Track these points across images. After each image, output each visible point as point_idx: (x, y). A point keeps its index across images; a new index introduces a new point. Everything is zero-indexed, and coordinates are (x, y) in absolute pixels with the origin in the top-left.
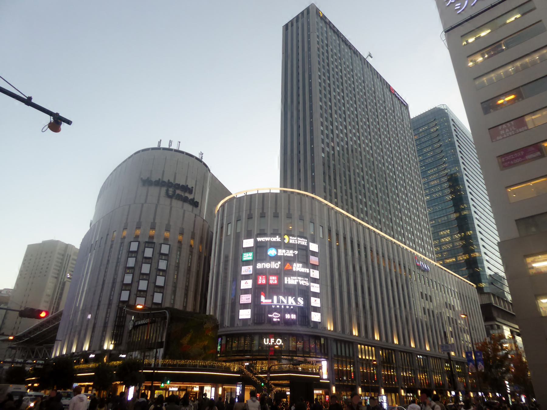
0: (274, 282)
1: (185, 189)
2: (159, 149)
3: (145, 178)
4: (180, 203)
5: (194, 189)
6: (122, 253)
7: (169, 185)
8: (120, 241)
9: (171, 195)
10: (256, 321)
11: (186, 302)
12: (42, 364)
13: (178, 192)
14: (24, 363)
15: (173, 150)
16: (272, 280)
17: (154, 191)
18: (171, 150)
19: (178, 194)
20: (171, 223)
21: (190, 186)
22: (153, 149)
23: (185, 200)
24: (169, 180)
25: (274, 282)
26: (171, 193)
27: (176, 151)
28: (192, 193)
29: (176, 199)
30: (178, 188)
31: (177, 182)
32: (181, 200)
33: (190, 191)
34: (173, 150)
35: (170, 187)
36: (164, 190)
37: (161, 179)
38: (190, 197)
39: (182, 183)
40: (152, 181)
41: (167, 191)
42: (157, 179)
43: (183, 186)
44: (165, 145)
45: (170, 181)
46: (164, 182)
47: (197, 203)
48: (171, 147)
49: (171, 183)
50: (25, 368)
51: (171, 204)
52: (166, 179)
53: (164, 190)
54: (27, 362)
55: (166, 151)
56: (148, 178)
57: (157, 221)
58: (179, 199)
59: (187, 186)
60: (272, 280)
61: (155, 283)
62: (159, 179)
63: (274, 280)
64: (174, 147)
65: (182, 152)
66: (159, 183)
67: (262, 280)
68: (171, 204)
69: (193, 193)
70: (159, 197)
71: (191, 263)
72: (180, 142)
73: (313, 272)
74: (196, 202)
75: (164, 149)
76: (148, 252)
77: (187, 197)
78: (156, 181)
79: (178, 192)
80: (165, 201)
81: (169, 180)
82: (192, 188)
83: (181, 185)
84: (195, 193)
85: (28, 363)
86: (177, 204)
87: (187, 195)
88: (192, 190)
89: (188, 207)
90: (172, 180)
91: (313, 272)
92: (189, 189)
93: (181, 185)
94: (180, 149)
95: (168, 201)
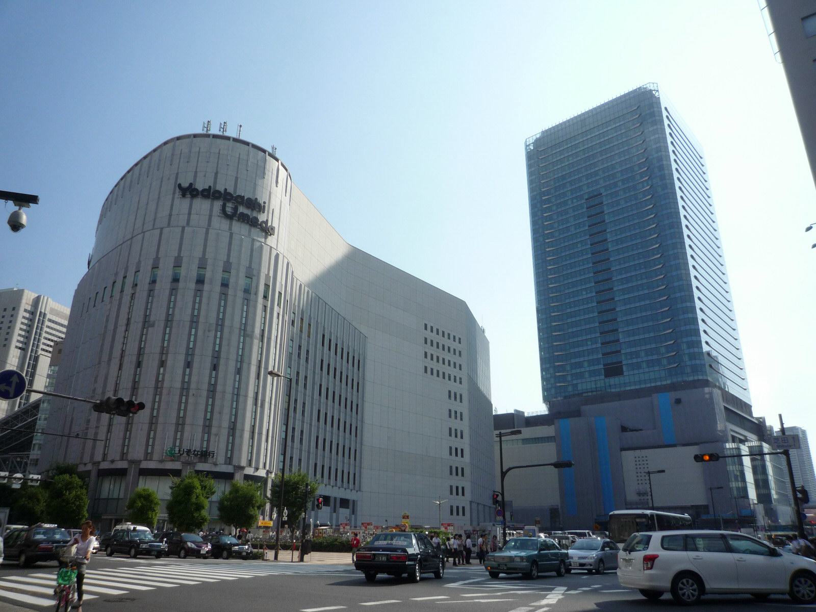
2: (208, 136)
3: (185, 185)
5: (266, 205)
6: (151, 308)
7: (226, 196)
8: (146, 287)
9: (229, 213)
12: (37, 480)
13: (241, 209)
14: (10, 478)
15: (231, 139)
17: (202, 206)
18: (228, 138)
19: (242, 214)
22: (195, 136)
24: (226, 190)
26: (229, 210)
27: (235, 140)
29: (239, 220)
31: (239, 192)
32: (248, 223)
34: (231, 139)
35: (229, 200)
36: (218, 204)
40: (197, 190)
41: (224, 206)
42: (207, 188)
43: (249, 199)
46: (219, 192)
48: (226, 134)
49: (230, 194)
50: (11, 486)
51: (230, 229)
52: (220, 188)
53: (218, 204)
54: (14, 476)
55: (219, 141)
56: (191, 184)
57: (209, 255)
58: (243, 221)
59: (256, 199)
62: (210, 187)
64: (231, 132)
65: (247, 144)
66: (209, 194)
68: (230, 229)
69: (266, 212)
70: (210, 216)
72: (241, 126)
75: (215, 136)
78: (204, 190)
79: (241, 209)
80: (220, 224)
81: (226, 190)
82: (265, 203)
85: (15, 478)
87: (255, 214)
88: (264, 206)
90: (231, 190)
92: (259, 205)
94: (242, 138)
95: (225, 224)
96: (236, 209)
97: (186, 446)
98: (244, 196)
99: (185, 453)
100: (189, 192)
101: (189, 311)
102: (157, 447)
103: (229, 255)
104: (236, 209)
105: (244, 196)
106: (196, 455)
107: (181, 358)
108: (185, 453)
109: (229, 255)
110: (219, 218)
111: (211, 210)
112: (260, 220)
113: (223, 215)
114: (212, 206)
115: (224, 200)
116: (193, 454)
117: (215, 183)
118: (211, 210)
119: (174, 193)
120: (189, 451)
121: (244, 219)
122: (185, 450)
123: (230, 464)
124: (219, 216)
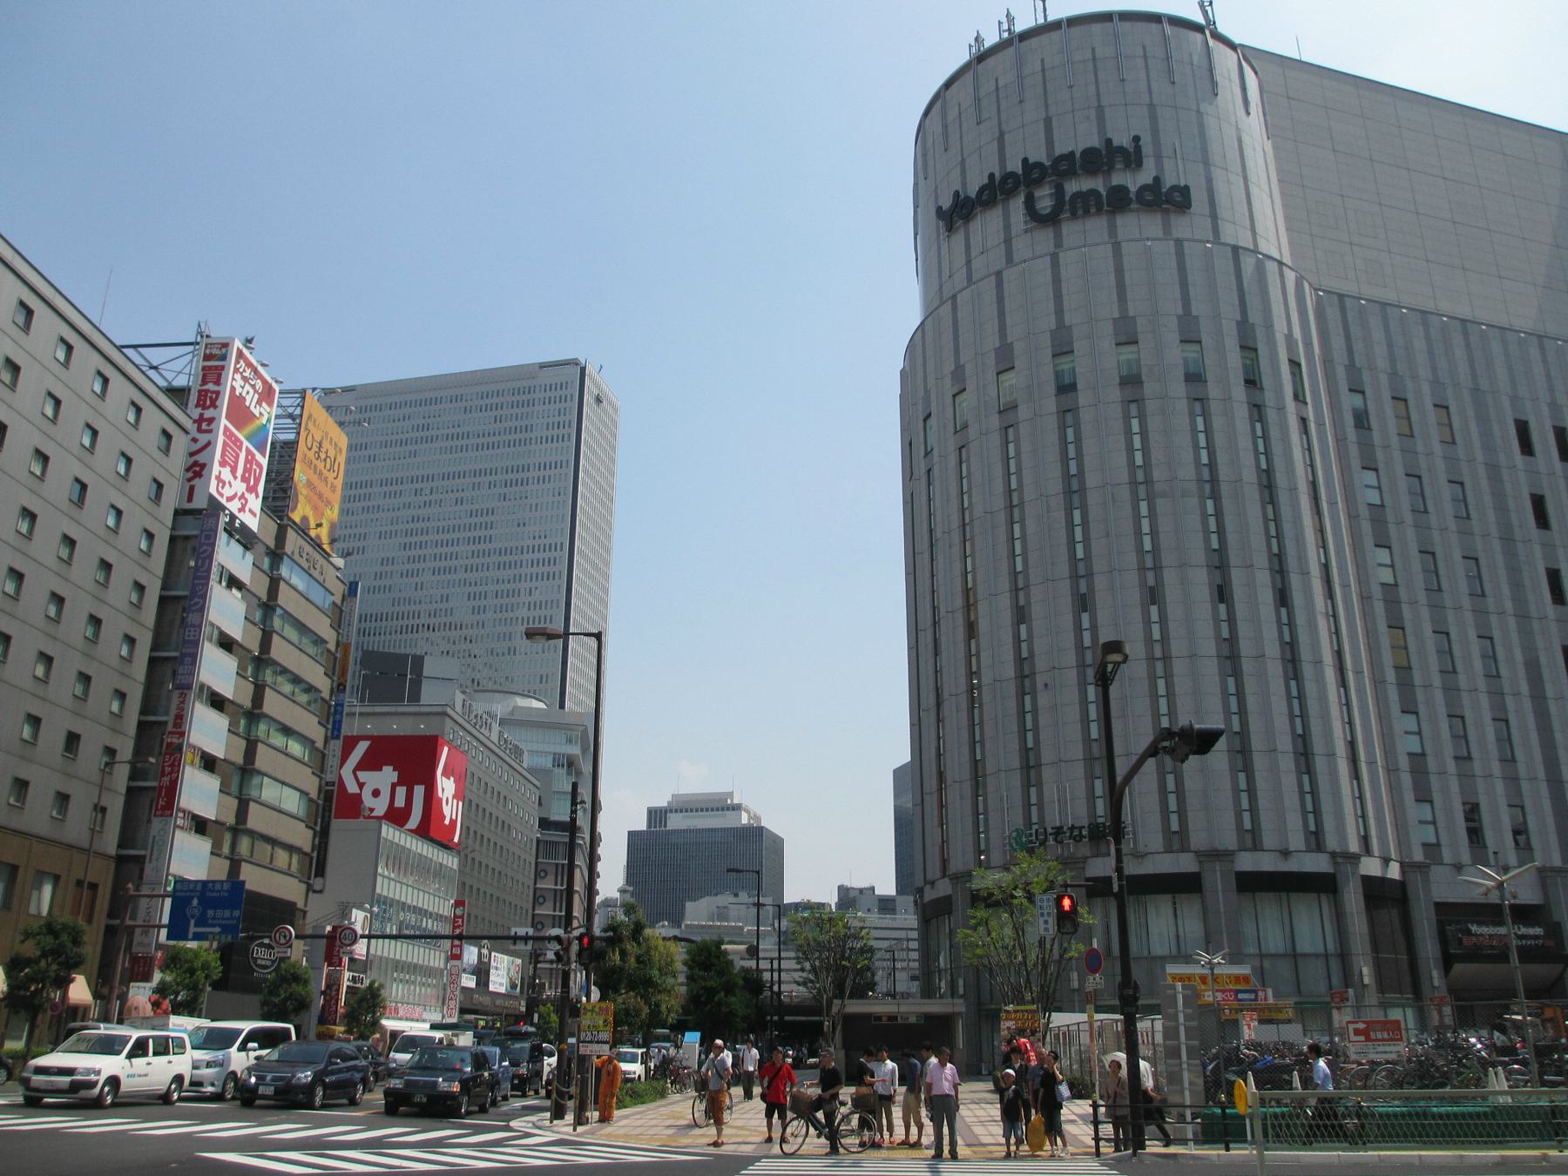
1: (1097, 159)
4: (1096, 227)
7: (1032, 174)
17: (988, 225)
19: (1077, 195)
20: (1068, 319)
21: (1122, 139)
23: (1118, 201)
24: (1025, 161)
29: (1074, 216)
30: (1071, 173)
32: (1099, 210)
33: (1132, 157)
35: (1038, 182)
36: (1017, 205)
37: (997, 175)
38: (1133, 181)
39: (1078, 137)
41: (1030, 203)
44: (991, 39)
45: (1031, 161)
46: (1013, 175)
49: (1038, 165)
53: (1017, 205)
58: (1087, 213)
62: (991, 176)
66: (997, 191)
74: (1175, 188)
79: (1072, 187)
80: (1033, 244)
81: (1025, 161)
83: (1078, 155)
88: (1138, 149)
89: (1138, 227)
90: (1038, 155)
92: (1121, 150)
93: (1078, 155)
95: (1044, 238)
96: (1059, 191)
97: (1053, 819)
98: (1072, 153)
99: (1051, 838)
101: (999, 486)
102: (993, 834)
104: (1059, 191)
106: (1078, 839)
107: (1005, 601)
108: (1051, 838)
109: (1059, 312)
110: (1029, 234)
111: (1007, 227)
112: (1133, 189)
113: (1034, 224)
115: (1027, 186)
116: (1070, 838)
118: (1007, 227)
120: (1058, 831)
121: (1086, 205)
122: (1049, 830)
123: (1184, 848)
124: (1026, 231)
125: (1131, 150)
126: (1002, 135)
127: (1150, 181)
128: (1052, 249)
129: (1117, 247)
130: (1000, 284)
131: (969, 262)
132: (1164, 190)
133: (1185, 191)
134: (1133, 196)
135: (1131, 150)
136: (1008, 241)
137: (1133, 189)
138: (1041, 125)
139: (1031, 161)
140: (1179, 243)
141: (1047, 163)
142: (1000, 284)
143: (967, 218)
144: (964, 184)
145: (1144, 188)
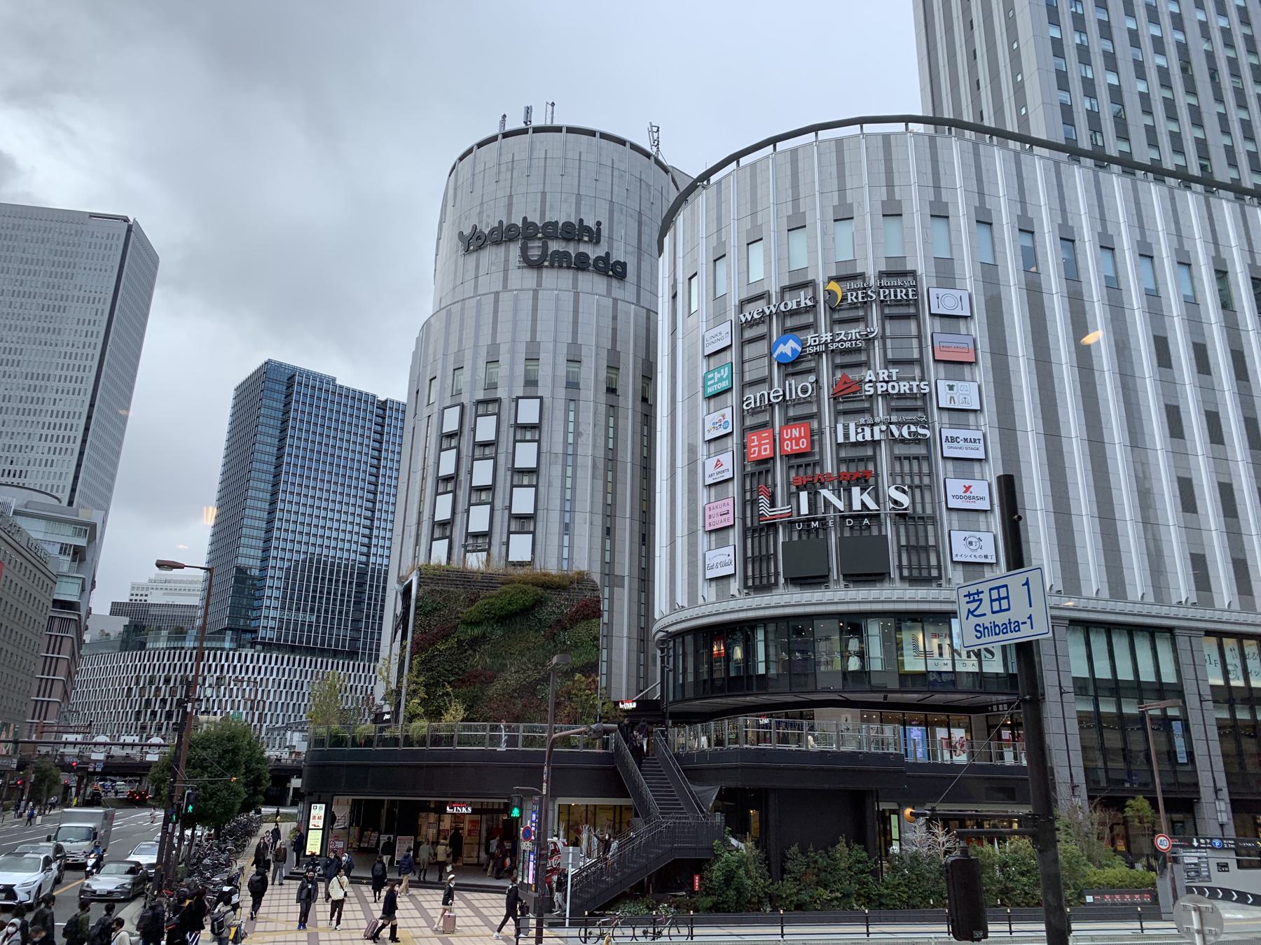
0: (797, 444)
1: (574, 232)
4: (565, 277)
10: (750, 583)
11: (612, 551)
13: (554, 246)
16: (790, 439)
17: (491, 256)
21: (590, 222)
23: (581, 264)
24: (525, 219)
25: (797, 444)
28: (598, 242)
29: (552, 266)
32: (569, 267)
33: (594, 236)
35: (532, 237)
36: (515, 250)
38: (593, 252)
39: (562, 214)
41: (524, 250)
43: (568, 224)
45: (529, 220)
46: (515, 226)
47: (624, 265)
49: (533, 224)
53: (515, 250)
60: (790, 439)
61: (492, 510)
62: (501, 222)
63: (797, 440)
66: (503, 235)
67: (760, 446)
70: (506, 271)
71: (615, 438)
73: (951, 388)
74: (618, 262)
76: (486, 429)
77: (583, 257)
78: (492, 232)
79: (554, 246)
81: (525, 219)
83: (560, 225)
84: (611, 238)
86: (557, 281)
88: (599, 230)
89: (591, 283)
90: (535, 218)
91: (951, 388)
92: (588, 229)
93: (560, 225)
95: (530, 277)
98: (557, 222)
100: (474, 242)
103: (534, 331)
105: (557, 222)
109: (534, 331)
111: (507, 261)
112: (592, 257)
114: (507, 253)
117: (509, 214)
118: (507, 261)
119: (457, 251)
121: (561, 261)
125: (595, 230)
126: (511, 196)
127: (603, 255)
128: (535, 287)
129: (577, 295)
130: (496, 301)
131: (477, 277)
132: (611, 262)
133: (624, 265)
134: (591, 262)
135: (595, 230)
136: (506, 271)
137: (592, 257)
138: (539, 195)
139: (529, 220)
140: (615, 300)
141: (540, 225)
142: (496, 301)
143: (480, 248)
144: (480, 222)
145: (599, 258)
